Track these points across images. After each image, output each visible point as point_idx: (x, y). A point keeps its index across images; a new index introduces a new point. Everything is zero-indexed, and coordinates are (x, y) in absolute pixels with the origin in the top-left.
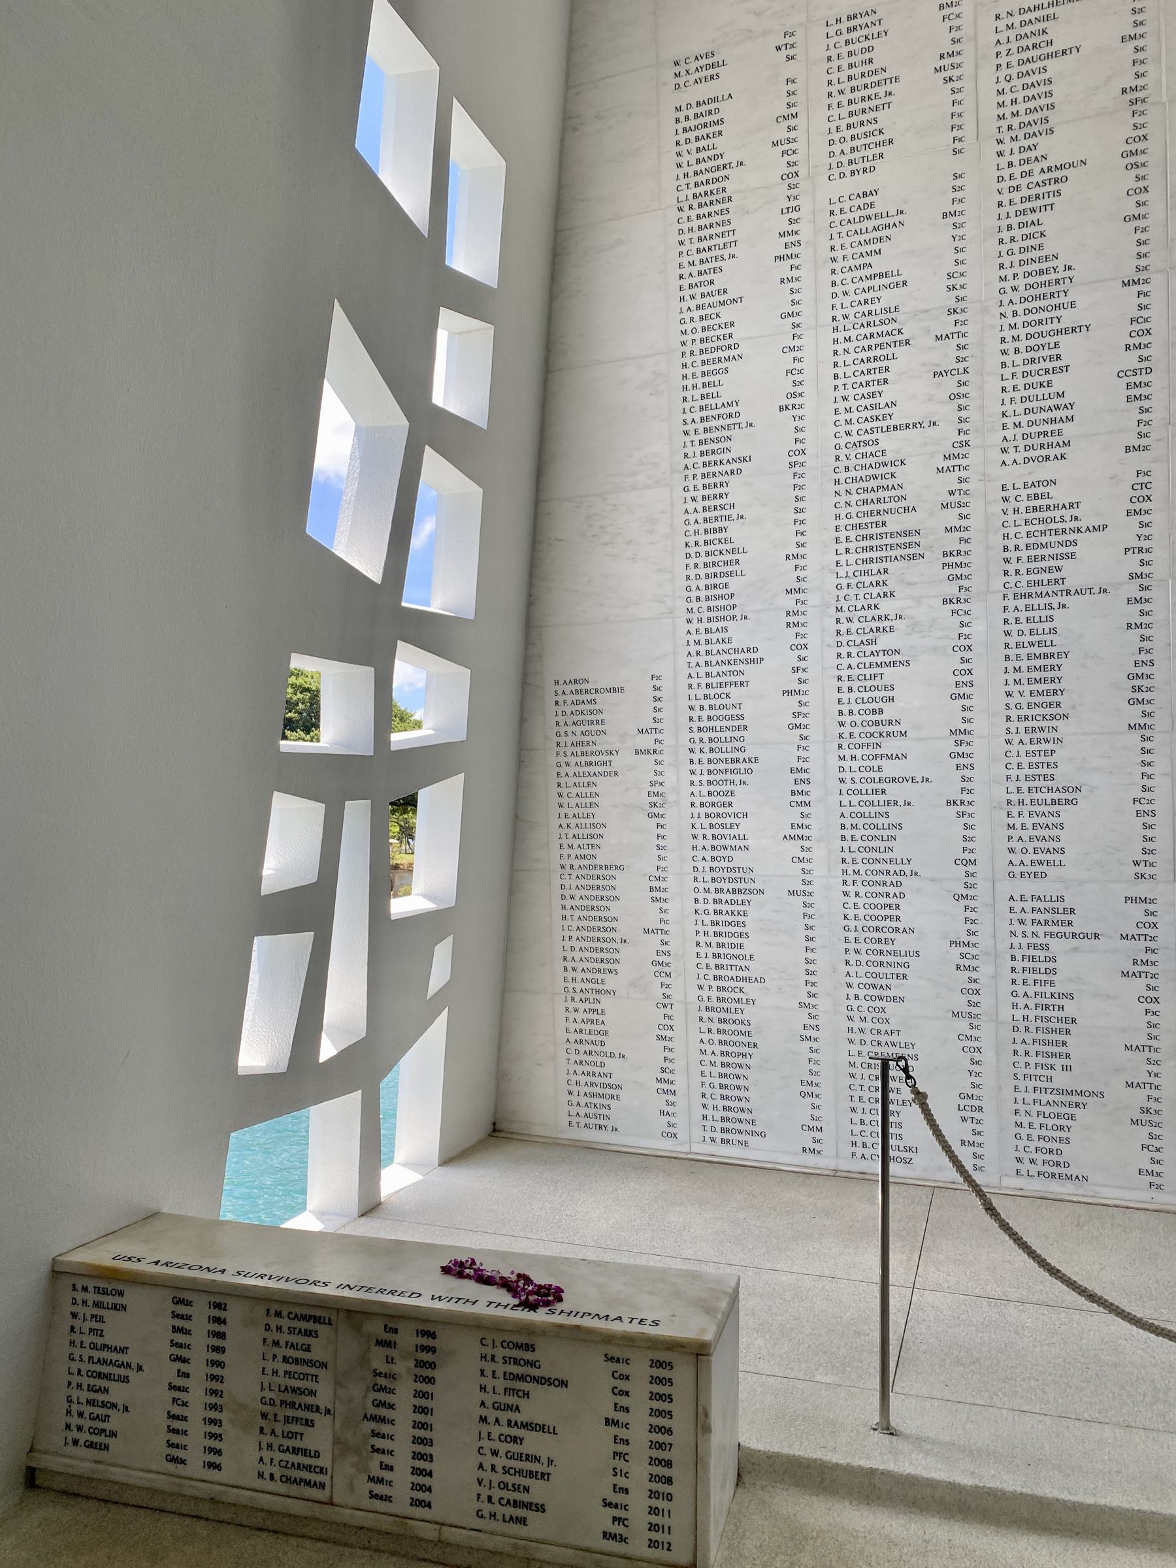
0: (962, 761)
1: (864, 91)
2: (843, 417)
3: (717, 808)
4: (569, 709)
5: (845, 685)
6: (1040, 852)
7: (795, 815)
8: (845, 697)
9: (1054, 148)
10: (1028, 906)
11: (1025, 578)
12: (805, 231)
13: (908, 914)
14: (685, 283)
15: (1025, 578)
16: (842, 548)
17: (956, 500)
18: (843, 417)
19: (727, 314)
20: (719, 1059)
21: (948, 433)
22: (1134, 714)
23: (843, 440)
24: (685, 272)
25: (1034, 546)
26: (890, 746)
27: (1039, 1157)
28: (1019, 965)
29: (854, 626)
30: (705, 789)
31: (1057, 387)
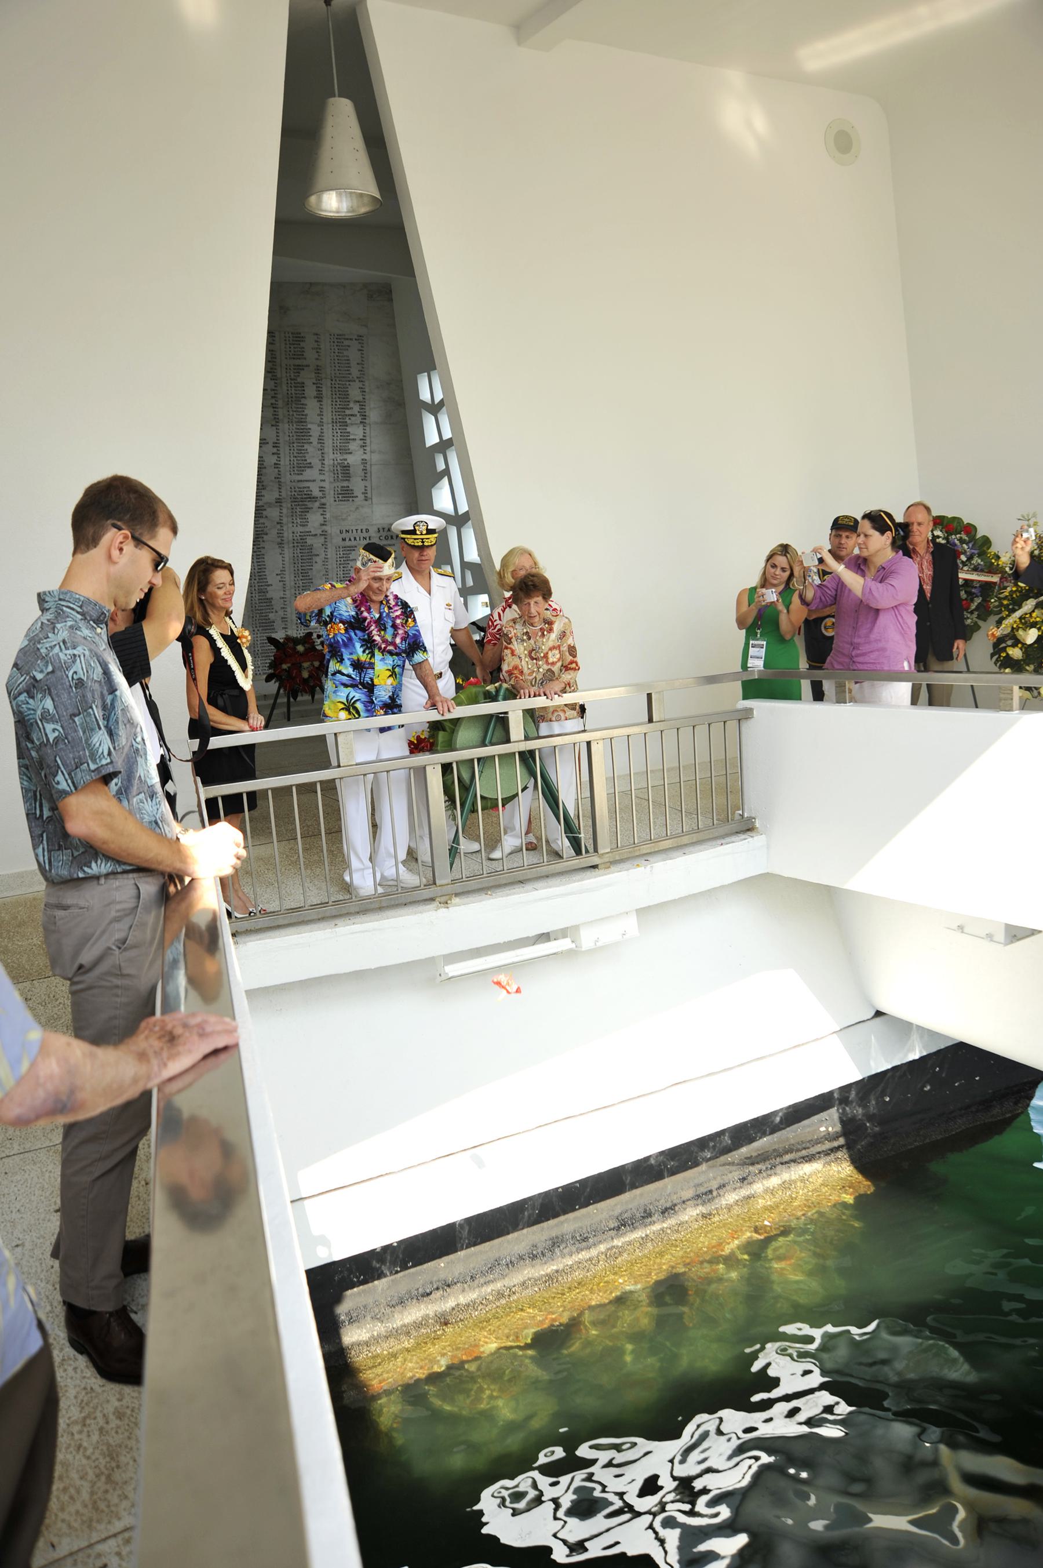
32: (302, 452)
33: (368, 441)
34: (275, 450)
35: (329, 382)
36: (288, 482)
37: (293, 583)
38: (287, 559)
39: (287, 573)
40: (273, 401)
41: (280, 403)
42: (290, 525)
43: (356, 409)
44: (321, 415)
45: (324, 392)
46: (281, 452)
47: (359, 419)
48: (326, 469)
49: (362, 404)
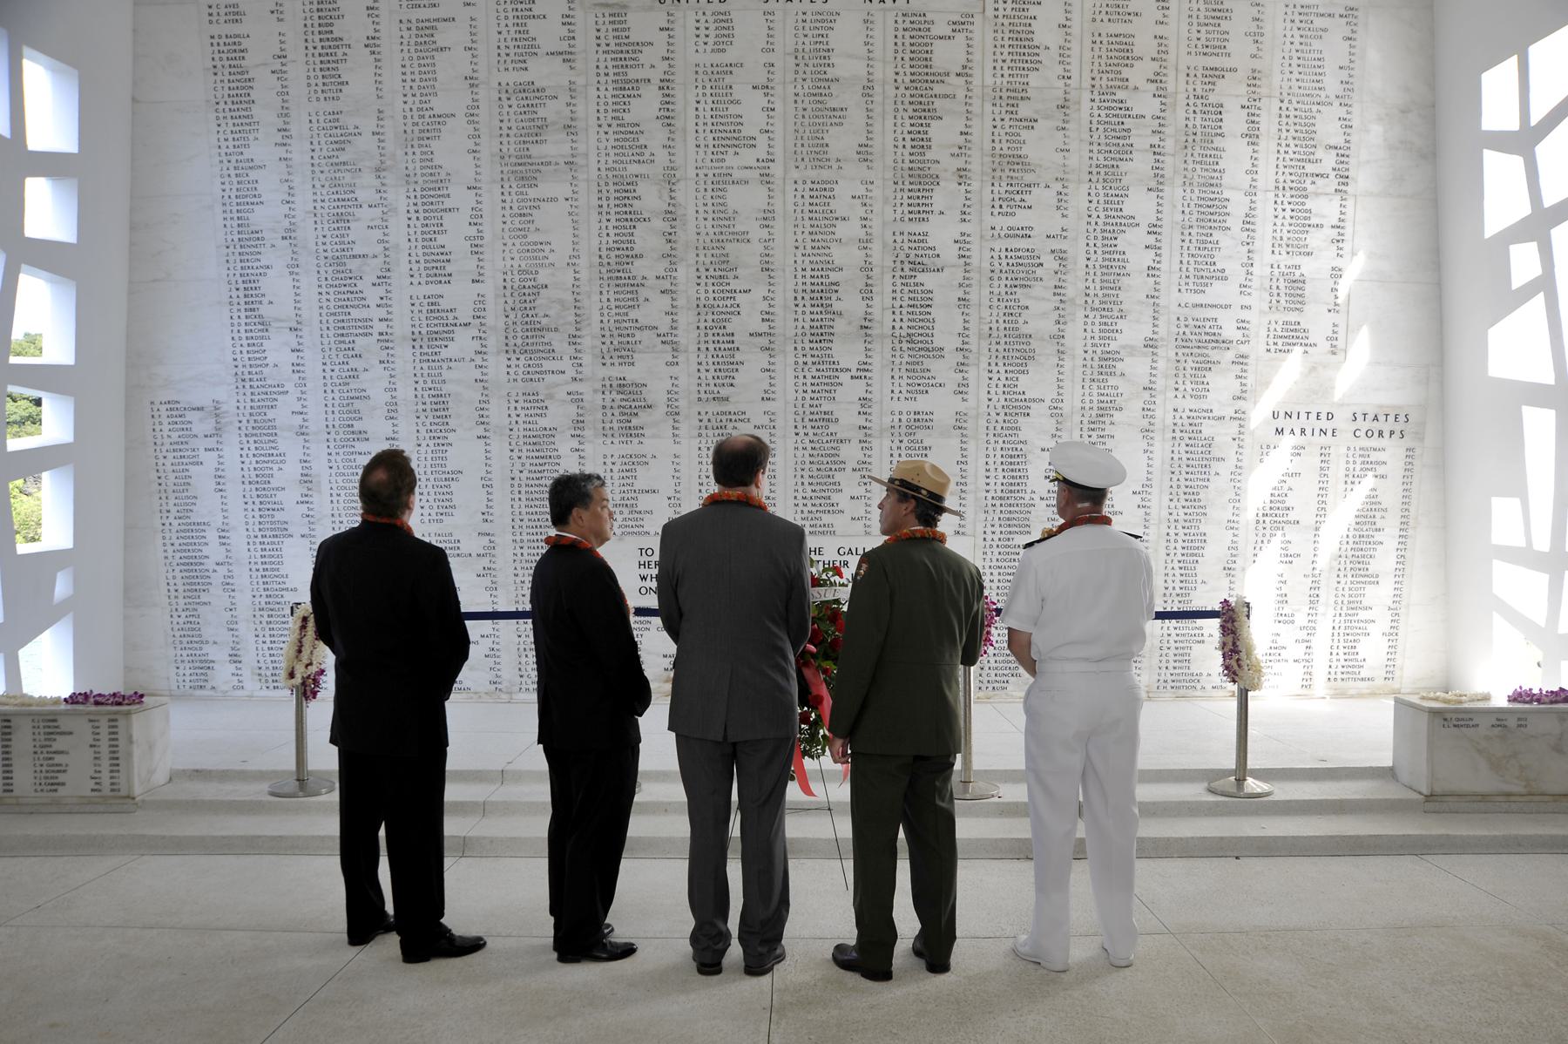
9: (439, 105)
32: (1207, 246)
33: (1348, 231)
34: (1151, 240)
35: (1276, 104)
36: (1174, 307)
37: (1165, 513)
38: (1157, 463)
39: (1155, 490)
40: (1155, 140)
41: (1169, 145)
42: (1171, 394)
43: (1329, 161)
44: (1252, 171)
45: (1263, 127)
46: (1165, 245)
47: (1333, 183)
48: (1255, 283)
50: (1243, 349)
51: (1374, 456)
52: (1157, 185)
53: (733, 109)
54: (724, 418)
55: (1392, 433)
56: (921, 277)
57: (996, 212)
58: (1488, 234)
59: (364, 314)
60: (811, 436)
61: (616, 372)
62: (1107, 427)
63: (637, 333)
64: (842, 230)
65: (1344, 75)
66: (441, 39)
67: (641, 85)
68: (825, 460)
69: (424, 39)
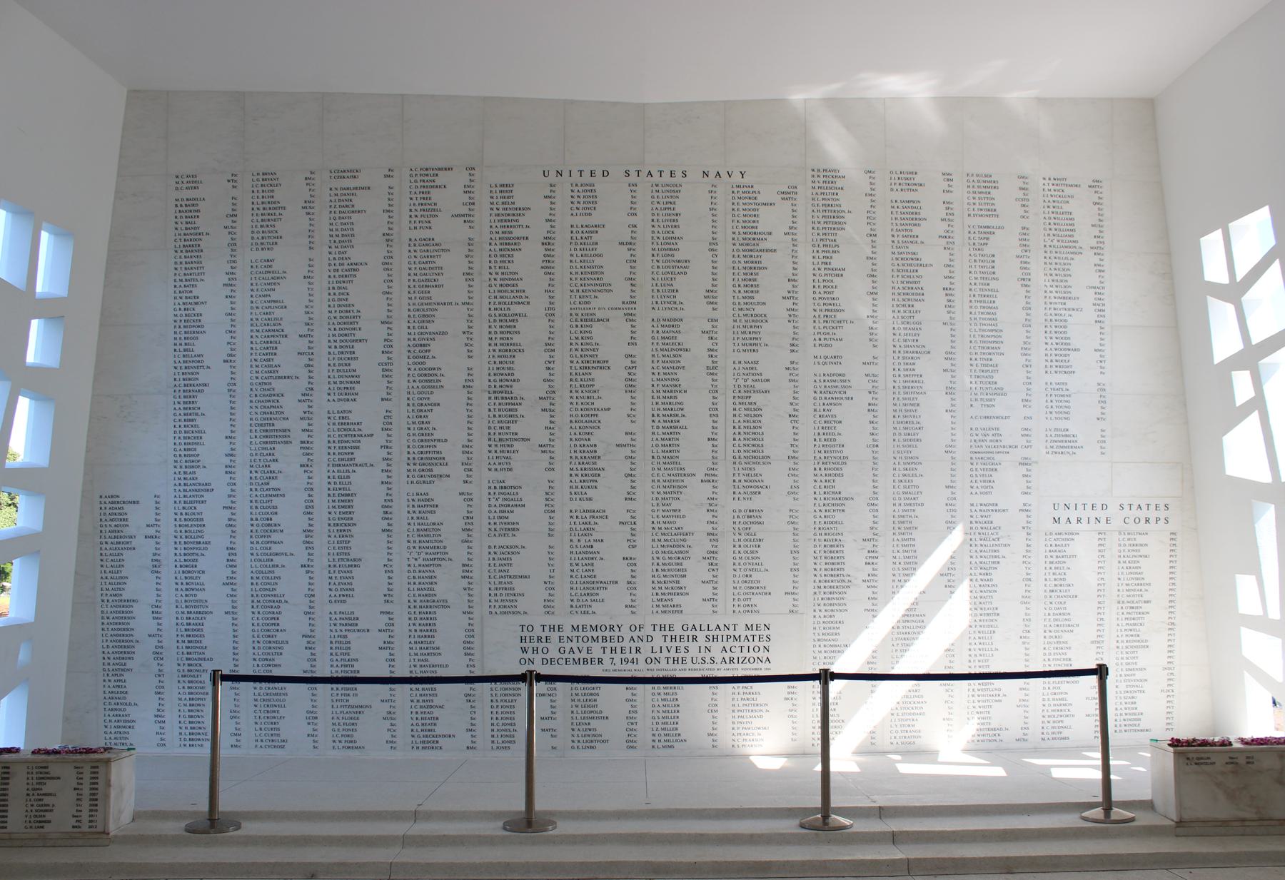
0: (309, 545)
1: (269, 211)
2: (255, 369)
3: (189, 568)
4: (108, 512)
5: (254, 505)
6: (344, 591)
7: (228, 572)
8: (254, 511)
9: (355, 255)
10: (338, 616)
11: (337, 457)
12: (239, 273)
13: (283, 622)
14: (178, 290)
15: (337, 457)
16: (253, 435)
17: (307, 416)
18: (255, 369)
19: (199, 309)
20: (188, 702)
21: (304, 383)
22: (384, 524)
23: (255, 381)
24: (178, 284)
25: (342, 442)
26: (275, 537)
27: (343, 739)
28: (334, 646)
29: (259, 475)
30: (183, 558)
31: (353, 367)
34: (947, 365)
49: (1098, 290)
50: (1027, 453)
51: (1140, 539)
52: (949, 323)
53: (598, 261)
54: (588, 515)
55: (1157, 520)
56: (755, 397)
57: (818, 342)
58: (1216, 361)
59: (285, 425)
60: (664, 531)
61: (500, 476)
62: (913, 520)
63: (517, 445)
64: (685, 359)
65: (1096, 231)
66: (358, 202)
67: (521, 241)
68: (674, 550)
69: (345, 204)
